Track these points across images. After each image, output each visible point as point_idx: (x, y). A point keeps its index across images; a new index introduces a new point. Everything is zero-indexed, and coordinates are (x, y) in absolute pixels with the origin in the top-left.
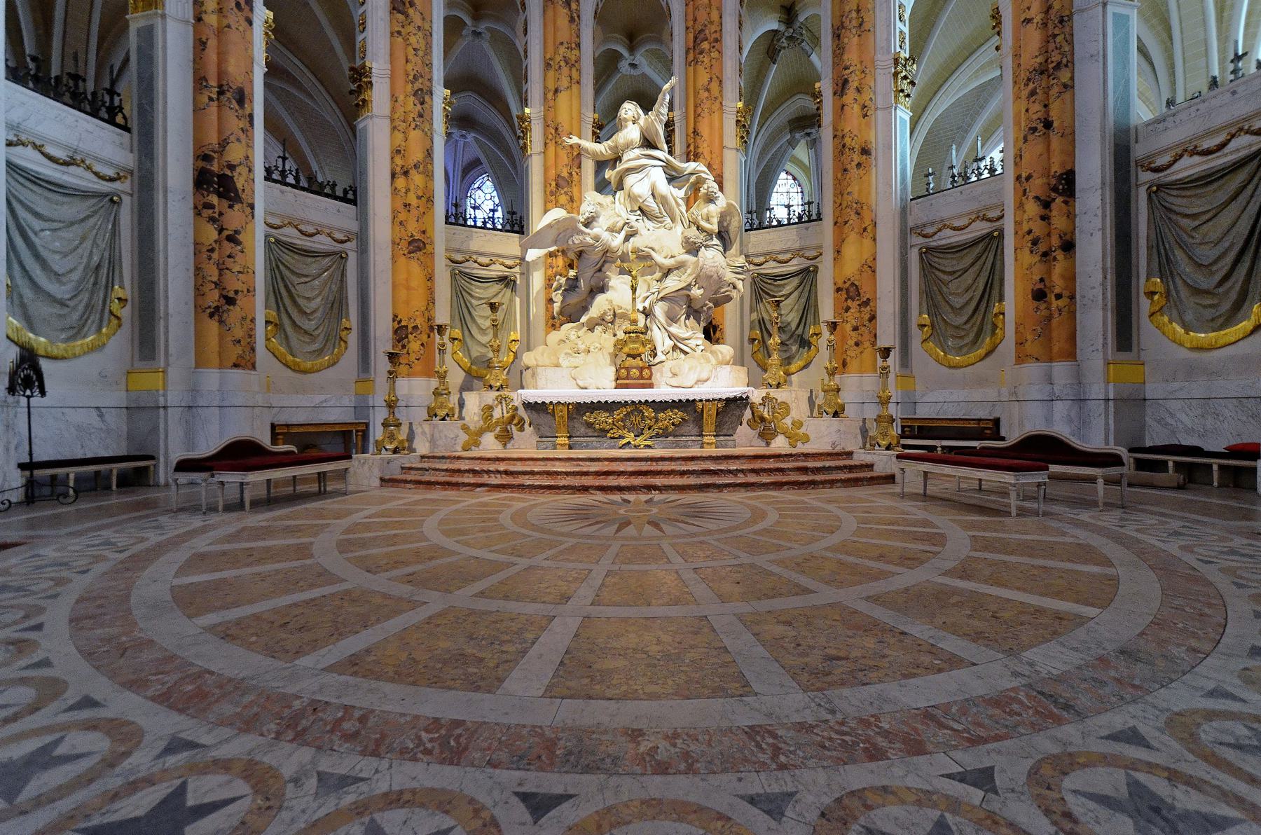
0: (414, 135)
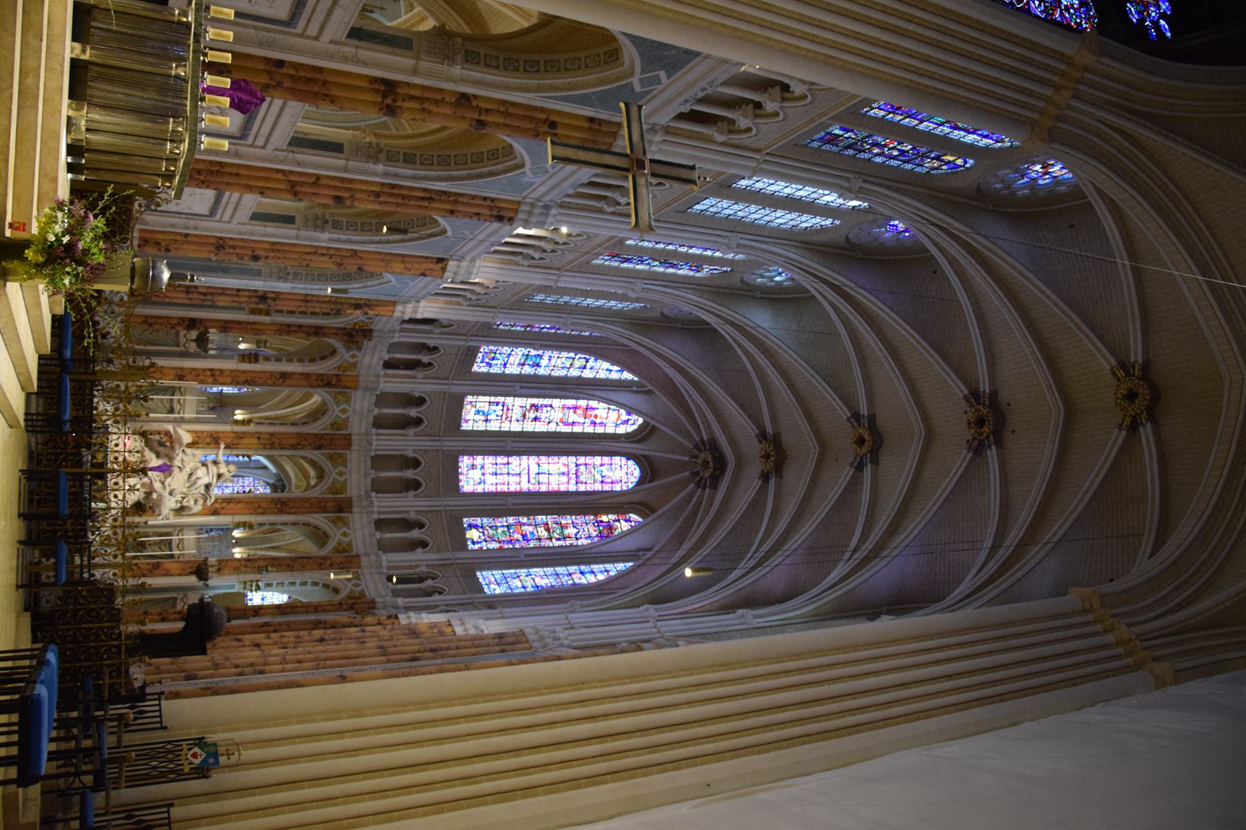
0: (229, 380)
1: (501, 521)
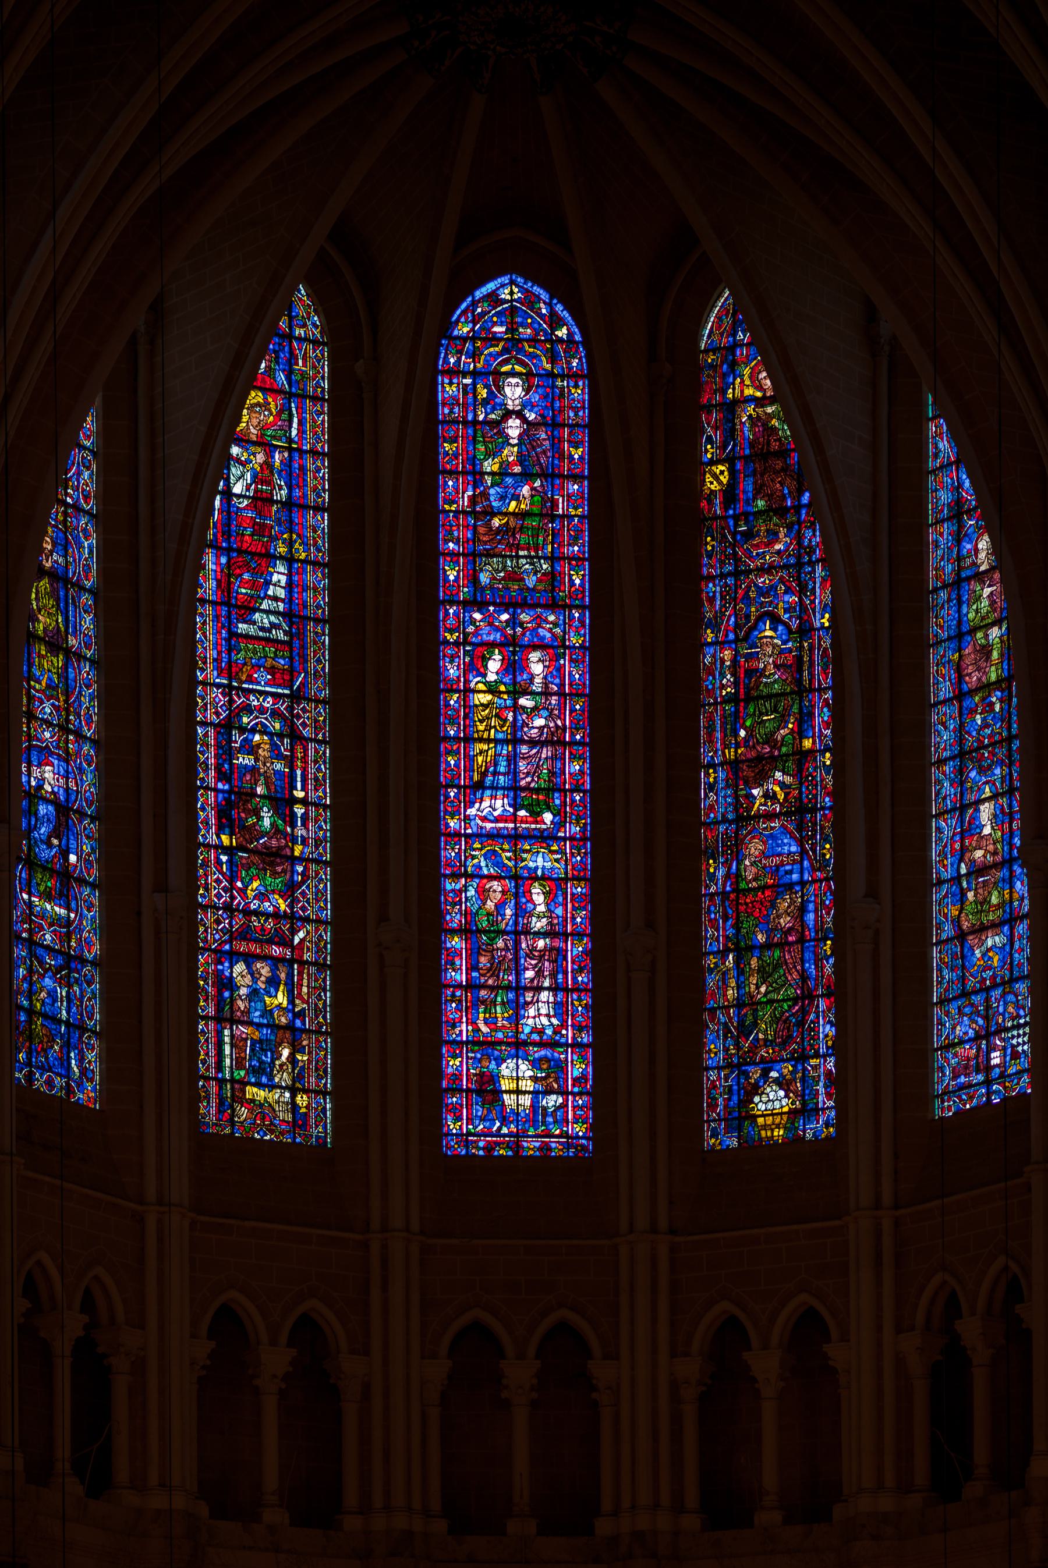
1: (724, 983)
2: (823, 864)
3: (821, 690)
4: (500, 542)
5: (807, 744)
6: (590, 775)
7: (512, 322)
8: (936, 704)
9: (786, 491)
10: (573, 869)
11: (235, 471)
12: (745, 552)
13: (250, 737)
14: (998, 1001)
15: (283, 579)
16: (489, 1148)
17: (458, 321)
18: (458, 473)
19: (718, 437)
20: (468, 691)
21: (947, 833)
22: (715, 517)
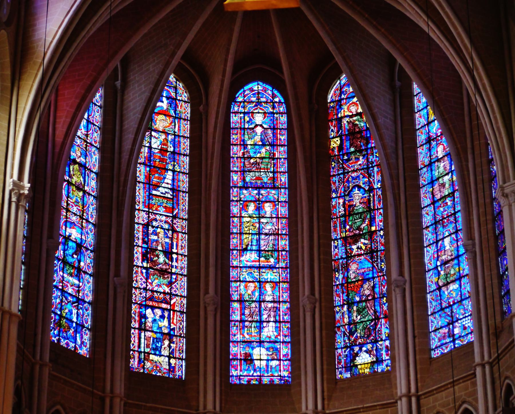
1: (342, 315)
2: (382, 270)
3: (378, 209)
4: (253, 167)
5: (373, 228)
6: (289, 245)
7: (258, 97)
8: (424, 207)
9: (362, 144)
10: (282, 278)
11: (153, 140)
12: (346, 166)
13: (156, 229)
14: (456, 309)
15: (171, 178)
16: (249, 381)
17: (238, 97)
18: (238, 145)
19: (335, 130)
20: (241, 217)
21: (431, 252)
22: (335, 155)
